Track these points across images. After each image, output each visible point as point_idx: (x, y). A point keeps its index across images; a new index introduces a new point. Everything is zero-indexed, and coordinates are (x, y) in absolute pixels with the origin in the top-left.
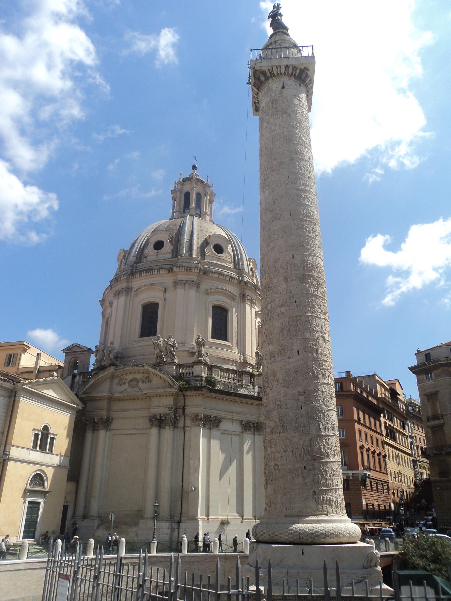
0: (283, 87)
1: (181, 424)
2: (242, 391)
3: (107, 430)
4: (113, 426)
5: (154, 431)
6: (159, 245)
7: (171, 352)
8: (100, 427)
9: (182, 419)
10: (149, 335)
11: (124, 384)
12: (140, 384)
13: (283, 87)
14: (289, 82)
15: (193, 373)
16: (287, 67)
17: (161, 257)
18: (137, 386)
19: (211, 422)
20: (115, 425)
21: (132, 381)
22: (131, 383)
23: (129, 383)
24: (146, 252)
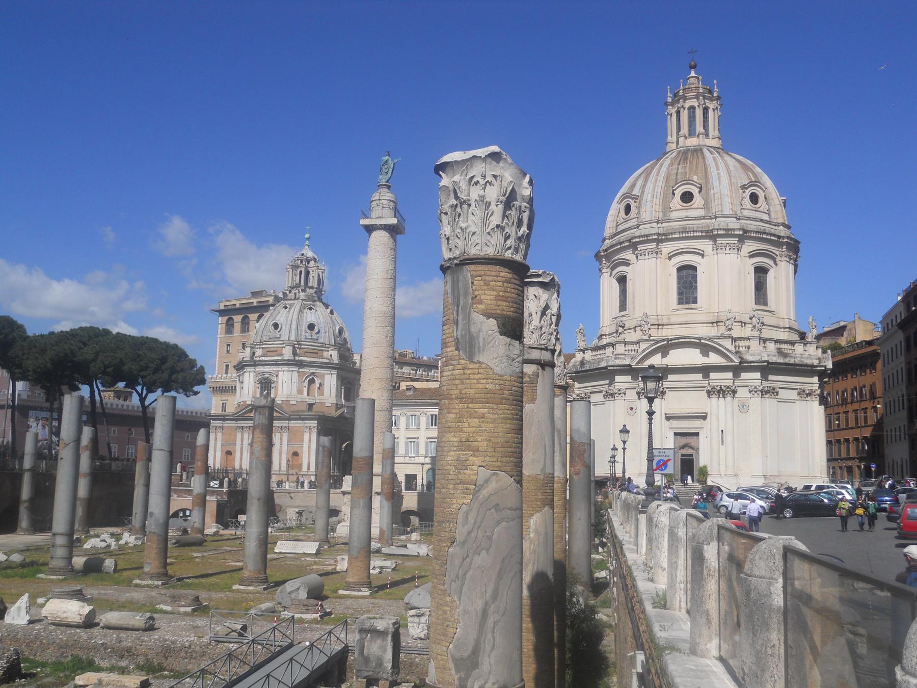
5: (714, 399)
10: (687, 303)
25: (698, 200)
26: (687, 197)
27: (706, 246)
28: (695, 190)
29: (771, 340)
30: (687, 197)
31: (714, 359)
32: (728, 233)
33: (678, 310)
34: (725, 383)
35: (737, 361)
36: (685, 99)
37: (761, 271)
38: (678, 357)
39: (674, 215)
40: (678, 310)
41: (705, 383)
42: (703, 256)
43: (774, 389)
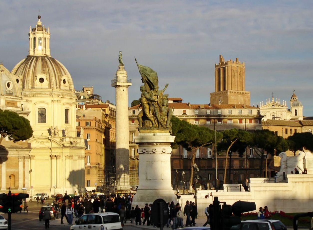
0: (124, 91)
1: (61, 158)
2: (78, 146)
3: (34, 159)
4: (35, 158)
6: (42, 80)
7: (57, 132)
11: (39, 143)
12: (45, 143)
13: (124, 91)
14: (125, 89)
16: (125, 86)
17: (43, 87)
18: (44, 144)
19: (71, 157)
21: (42, 142)
22: (41, 143)
23: (41, 143)
24: (35, 82)
25: (46, 82)
26: (42, 80)
27: (49, 100)
29: (72, 138)
34: (57, 154)
37: (67, 111)
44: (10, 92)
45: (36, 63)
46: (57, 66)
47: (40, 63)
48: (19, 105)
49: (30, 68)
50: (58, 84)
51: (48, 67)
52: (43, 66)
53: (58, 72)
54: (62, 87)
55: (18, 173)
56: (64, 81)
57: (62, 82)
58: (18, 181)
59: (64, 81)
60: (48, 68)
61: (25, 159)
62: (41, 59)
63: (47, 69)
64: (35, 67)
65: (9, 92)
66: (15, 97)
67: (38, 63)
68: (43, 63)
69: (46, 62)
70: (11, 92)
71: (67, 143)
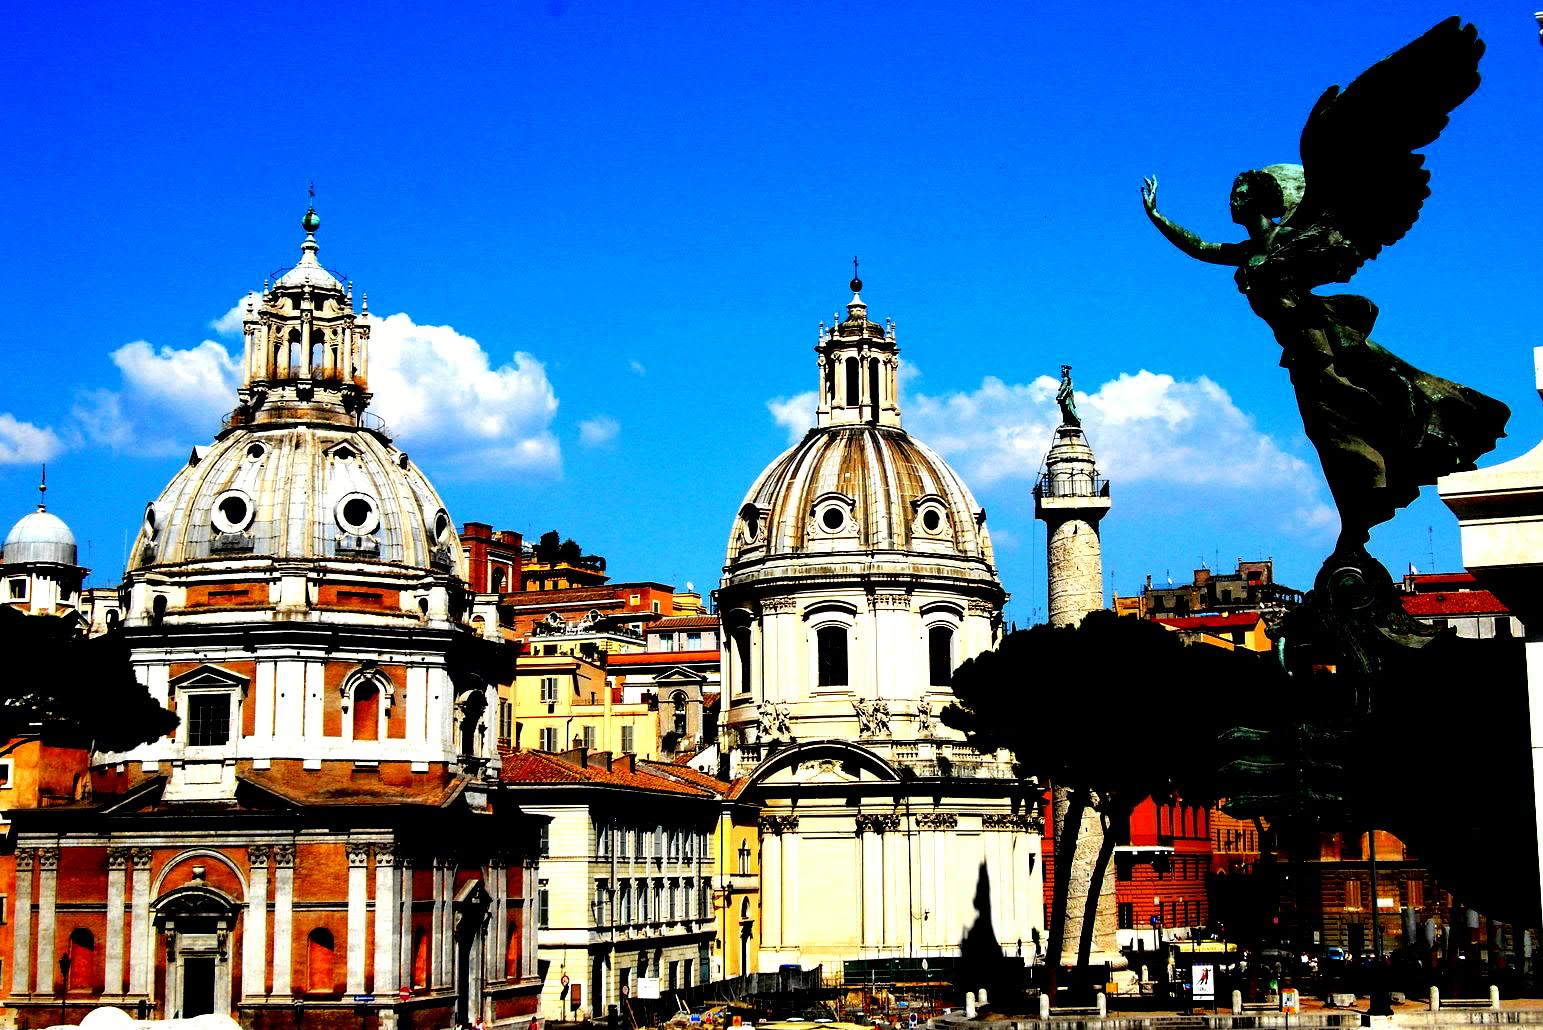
0: (1075, 532)
1: (903, 826)
5: (870, 836)
7: (884, 725)
8: (785, 830)
9: (904, 820)
11: (812, 767)
13: (1075, 532)
14: (1082, 525)
15: (917, 754)
19: (946, 822)
20: (804, 825)
24: (809, 529)
25: (849, 526)
26: (833, 519)
27: (857, 597)
28: (845, 510)
30: (833, 519)
31: (867, 776)
32: (892, 581)
33: (820, 694)
35: (897, 780)
36: (843, 346)
38: (810, 774)
39: (812, 547)
40: (820, 694)
41: (853, 810)
42: (854, 613)
43: (952, 816)
44: (359, 545)
45: (822, 455)
46: (907, 459)
47: (838, 451)
48: (408, 601)
49: (794, 476)
50: (899, 529)
51: (864, 465)
52: (846, 461)
53: (906, 481)
54: (917, 546)
55: (344, 921)
56: (931, 520)
57: (919, 525)
58: (342, 959)
59: (931, 520)
60: (863, 471)
61: (379, 857)
62: (844, 441)
63: (860, 472)
64: (816, 470)
65: (353, 545)
66: (387, 569)
67: (829, 453)
68: (849, 453)
69: (862, 449)
70: (366, 545)
71: (924, 763)
